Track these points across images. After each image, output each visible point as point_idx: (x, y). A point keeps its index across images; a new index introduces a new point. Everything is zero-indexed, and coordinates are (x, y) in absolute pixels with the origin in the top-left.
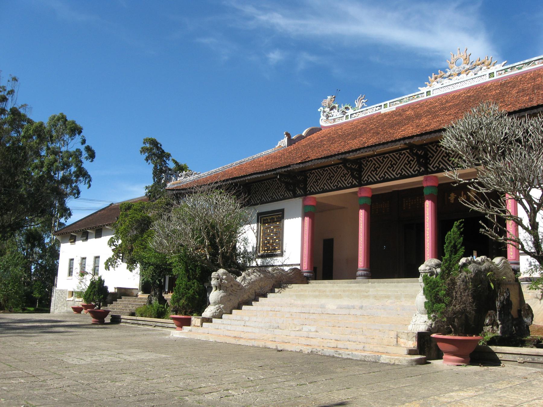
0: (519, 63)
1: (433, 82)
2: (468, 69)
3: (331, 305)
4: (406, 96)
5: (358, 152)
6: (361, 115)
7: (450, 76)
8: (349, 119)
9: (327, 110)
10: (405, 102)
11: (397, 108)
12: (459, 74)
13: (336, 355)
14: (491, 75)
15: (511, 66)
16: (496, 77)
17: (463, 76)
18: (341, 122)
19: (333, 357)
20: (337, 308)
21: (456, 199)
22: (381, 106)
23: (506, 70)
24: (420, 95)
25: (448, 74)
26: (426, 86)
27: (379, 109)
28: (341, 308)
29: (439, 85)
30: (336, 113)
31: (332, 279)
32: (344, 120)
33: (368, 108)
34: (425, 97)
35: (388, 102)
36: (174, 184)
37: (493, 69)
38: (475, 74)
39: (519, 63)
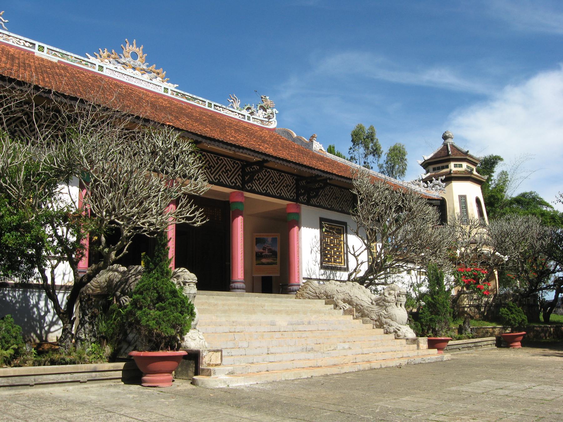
0: (188, 94)
1: (105, 58)
2: (144, 70)
3: (282, 321)
4: (72, 55)
5: (241, 150)
7: (124, 64)
10: (68, 59)
11: (59, 61)
13: (422, 362)
14: (166, 89)
15: (183, 92)
16: (169, 94)
17: (137, 74)
19: (421, 363)
20: (288, 325)
22: (34, 44)
23: (178, 93)
24: (89, 64)
25: (123, 60)
27: (29, 47)
28: (292, 324)
29: (111, 66)
31: (272, 293)
33: (11, 34)
34: (96, 70)
35: (46, 46)
37: (166, 85)
38: (151, 79)
39: (188, 94)
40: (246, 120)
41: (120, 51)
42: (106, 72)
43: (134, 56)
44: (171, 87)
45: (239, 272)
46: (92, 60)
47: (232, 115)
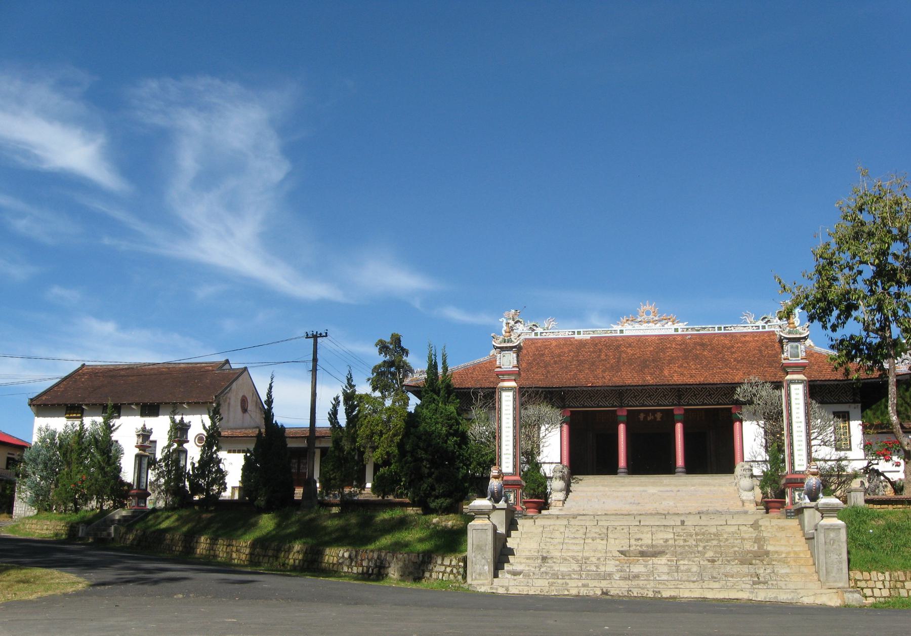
3: (652, 490)
6: (552, 336)
8: (539, 337)
9: (512, 323)
12: (649, 322)
14: (676, 330)
16: (680, 332)
18: (528, 337)
21: (645, 418)
23: (687, 329)
26: (618, 324)
29: (630, 327)
30: (520, 328)
32: (533, 336)
34: (619, 334)
36: (412, 381)
37: (676, 326)
40: (761, 330)
41: (636, 314)
42: (626, 333)
43: (648, 313)
44: (680, 326)
45: (680, 461)
46: (616, 327)
47: (745, 330)
